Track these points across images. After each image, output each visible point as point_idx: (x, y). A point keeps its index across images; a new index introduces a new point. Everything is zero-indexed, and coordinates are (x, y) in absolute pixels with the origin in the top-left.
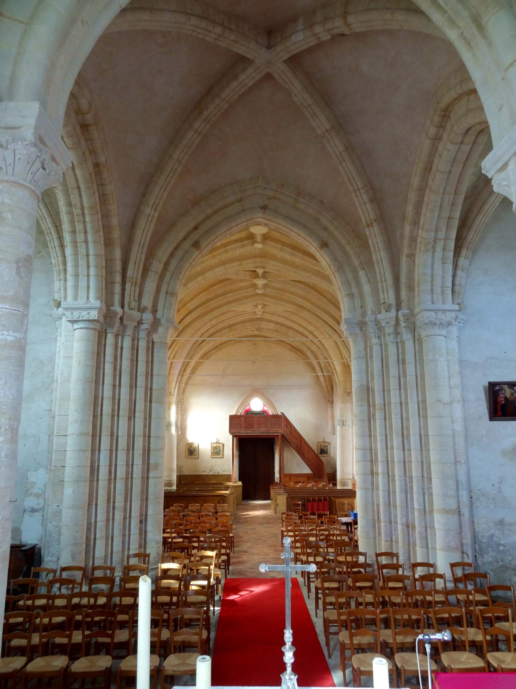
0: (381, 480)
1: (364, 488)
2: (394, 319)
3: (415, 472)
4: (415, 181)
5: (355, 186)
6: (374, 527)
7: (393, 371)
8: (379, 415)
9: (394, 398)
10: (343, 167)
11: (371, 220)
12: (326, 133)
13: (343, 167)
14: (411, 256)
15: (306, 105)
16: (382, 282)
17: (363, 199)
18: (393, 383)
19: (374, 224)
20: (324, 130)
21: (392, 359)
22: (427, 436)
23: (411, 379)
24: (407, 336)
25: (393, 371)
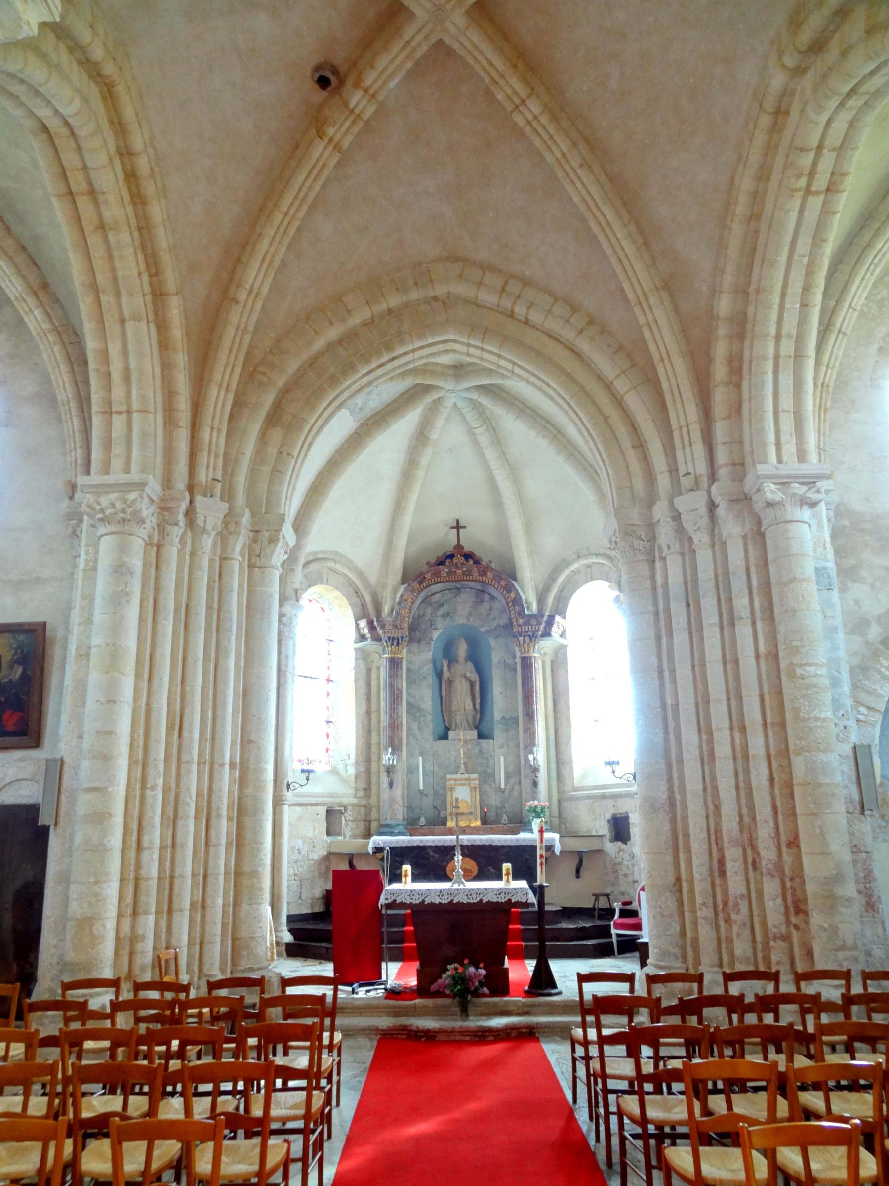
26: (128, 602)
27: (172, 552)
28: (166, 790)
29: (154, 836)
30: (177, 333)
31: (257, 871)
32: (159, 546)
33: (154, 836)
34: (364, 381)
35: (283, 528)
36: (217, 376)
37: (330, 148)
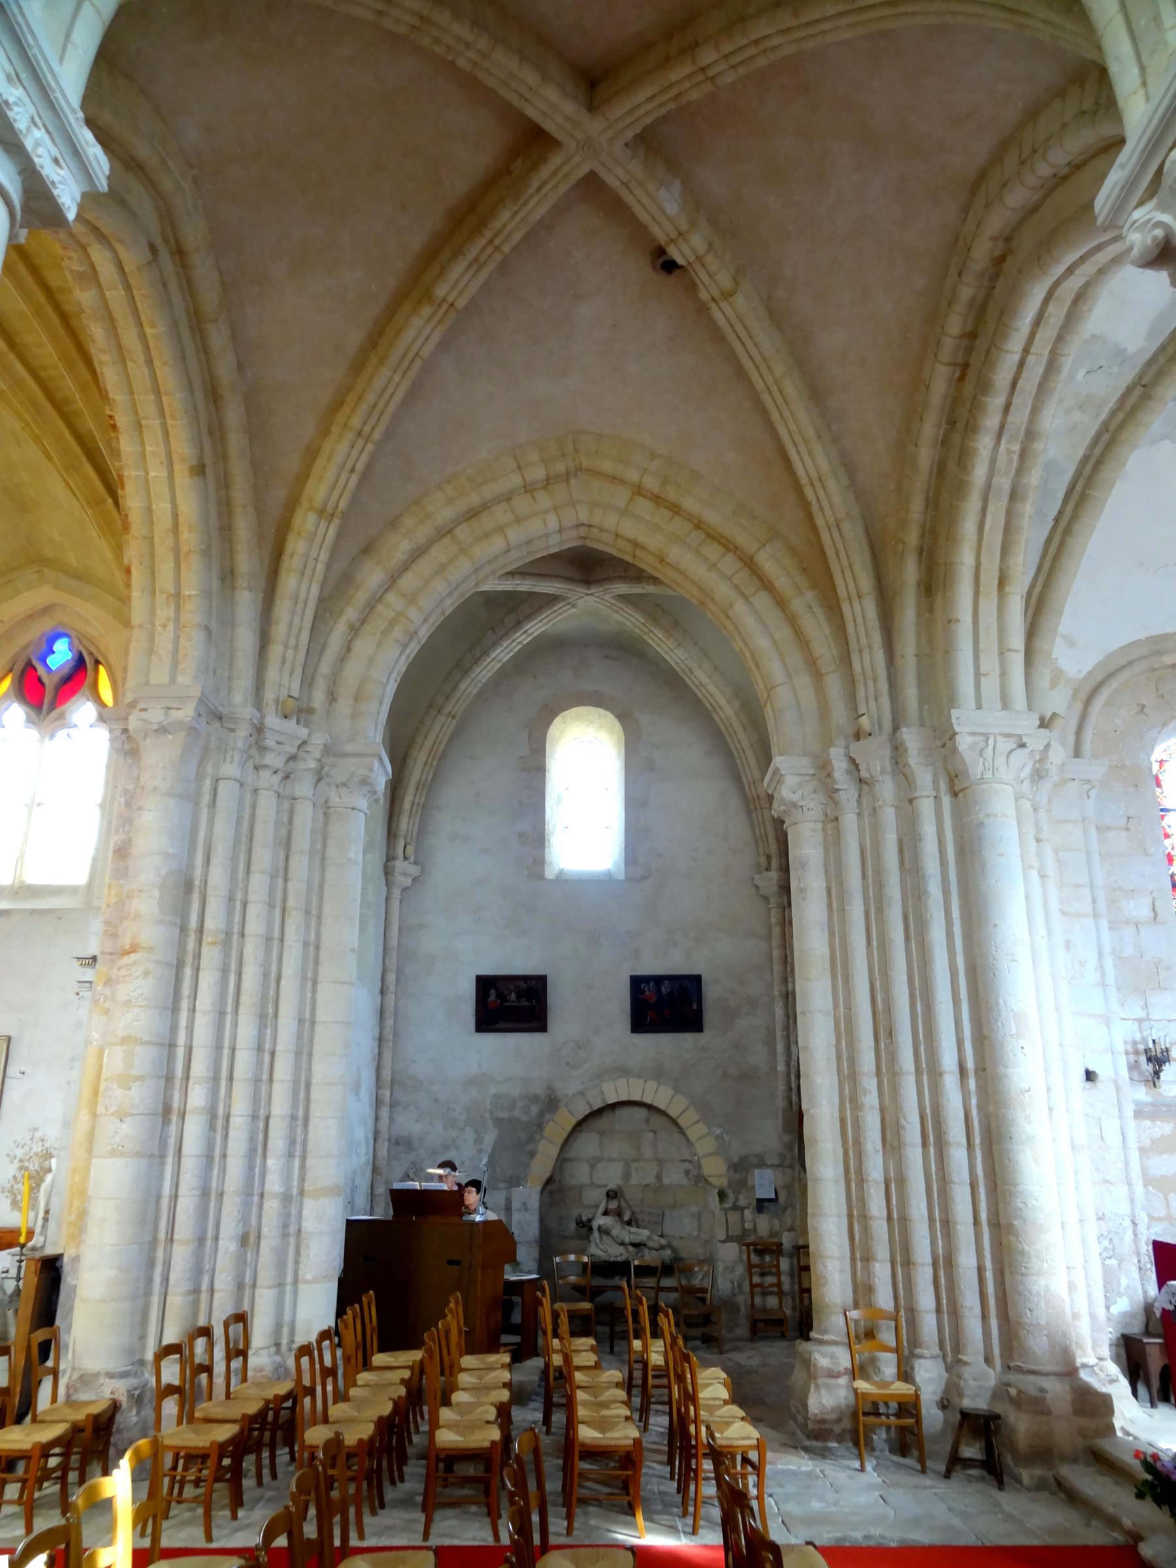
0: (194, 1130)
1: (149, 1153)
2: (299, 742)
3: (280, 1106)
4: (445, 515)
5: (367, 429)
6: (151, 1264)
7: (263, 856)
8: (211, 956)
9: (255, 927)
10: (390, 379)
11: (336, 507)
12: (445, 307)
13: (390, 379)
14: (355, 630)
15: (497, 242)
16: (286, 647)
17: (358, 460)
18: (258, 884)
19: (336, 522)
20: (451, 299)
21: (265, 831)
22: (313, 1022)
23: (297, 887)
24: (303, 788)
25: (263, 856)
26: (804, 899)
27: (850, 821)
28: (882, 1110)
29: (875, 1167)
30: (781, 582)
31: (1013, 1225)
32: (837, 819)
33: (875, 1167)
34: (1011, 447)
35: (957, 728)
36: (841, 591)
37: (724, 305)
